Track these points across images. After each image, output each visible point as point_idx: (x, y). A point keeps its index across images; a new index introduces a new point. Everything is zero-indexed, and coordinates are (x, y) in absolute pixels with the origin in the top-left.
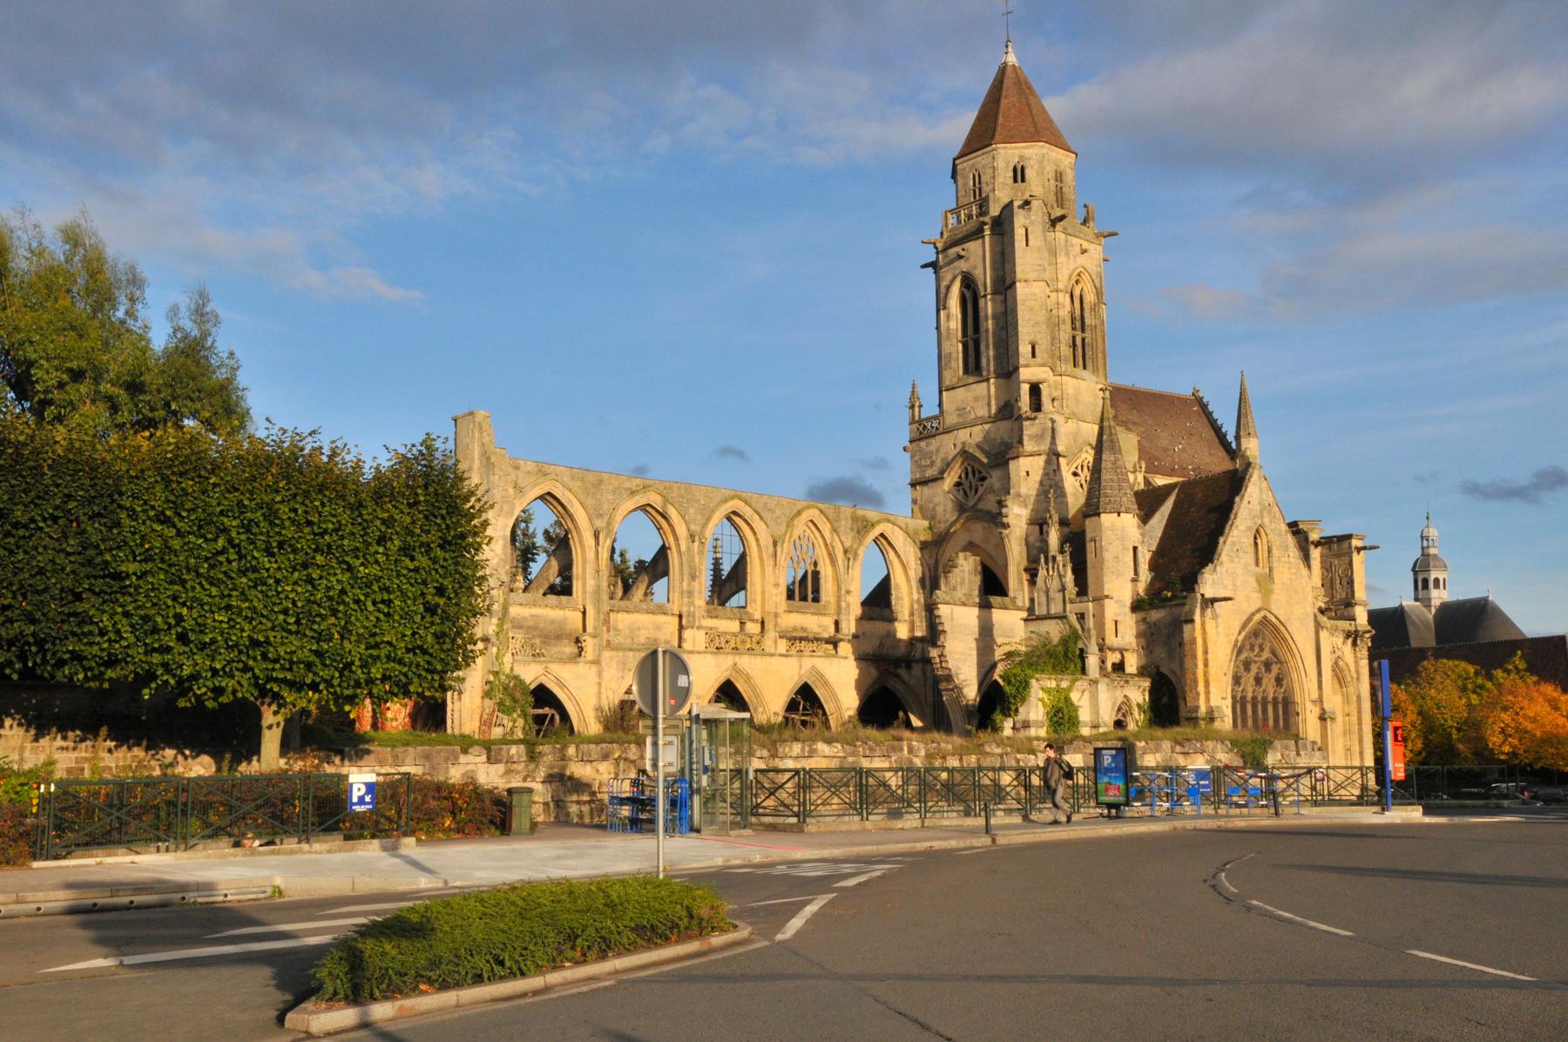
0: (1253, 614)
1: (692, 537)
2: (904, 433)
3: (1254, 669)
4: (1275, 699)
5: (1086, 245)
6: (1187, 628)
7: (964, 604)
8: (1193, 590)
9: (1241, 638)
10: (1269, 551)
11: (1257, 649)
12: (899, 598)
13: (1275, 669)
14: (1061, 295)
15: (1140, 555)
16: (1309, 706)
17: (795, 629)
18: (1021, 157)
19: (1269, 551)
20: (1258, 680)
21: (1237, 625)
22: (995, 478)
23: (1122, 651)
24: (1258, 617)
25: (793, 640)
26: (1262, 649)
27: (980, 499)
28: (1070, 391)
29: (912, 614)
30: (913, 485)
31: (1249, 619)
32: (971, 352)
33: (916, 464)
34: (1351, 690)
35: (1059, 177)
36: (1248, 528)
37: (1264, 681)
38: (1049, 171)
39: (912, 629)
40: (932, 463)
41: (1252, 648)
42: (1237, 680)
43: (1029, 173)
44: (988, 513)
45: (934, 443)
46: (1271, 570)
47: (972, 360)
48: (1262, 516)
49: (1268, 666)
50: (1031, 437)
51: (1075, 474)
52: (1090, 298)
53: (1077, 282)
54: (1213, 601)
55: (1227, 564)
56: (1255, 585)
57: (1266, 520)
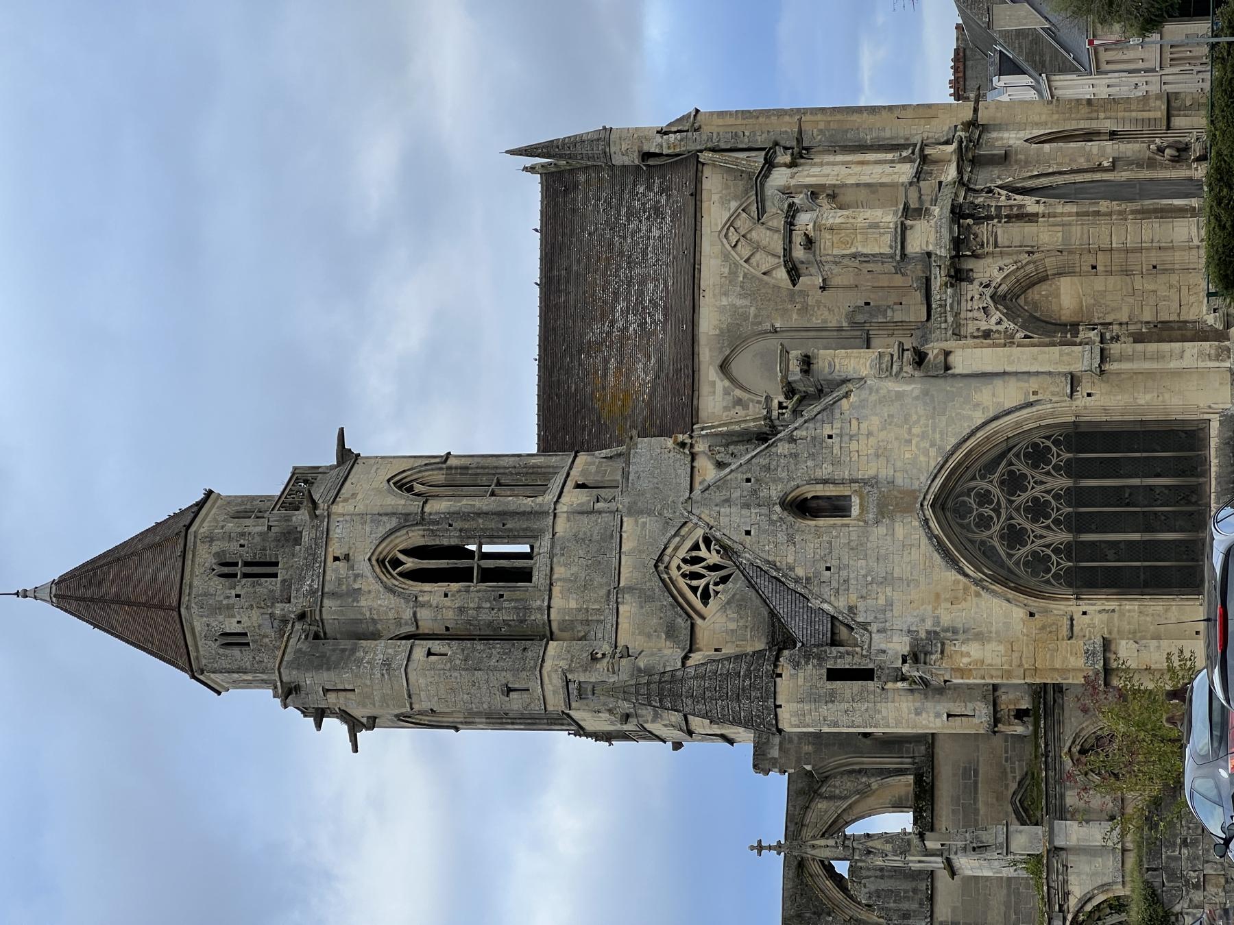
0: (931, 536)
3: (1021, 521)
4: (1070, 469)
5: (335, 549)
7: (931, 899)
9: (969, 570)
10: (825, 482)
11: (987, 511)
13: (1021, 467)
15: (840, 664)
16: (1081, 401)
19: (825, 482)
20: (1037, 510)
21: (952, 575)
24: (934, 524)
26: (984, 498)
28: (573, 604)
34: (1050, 263)
35: (227, 569)
36: (791, 540)
37: (1037, 491)
48: (768, 504)
49: (1014, 483)
52: (416, 538)
53: (396, 563)
55: (853, 599)
56: (882, 530)
57: (775, 492)
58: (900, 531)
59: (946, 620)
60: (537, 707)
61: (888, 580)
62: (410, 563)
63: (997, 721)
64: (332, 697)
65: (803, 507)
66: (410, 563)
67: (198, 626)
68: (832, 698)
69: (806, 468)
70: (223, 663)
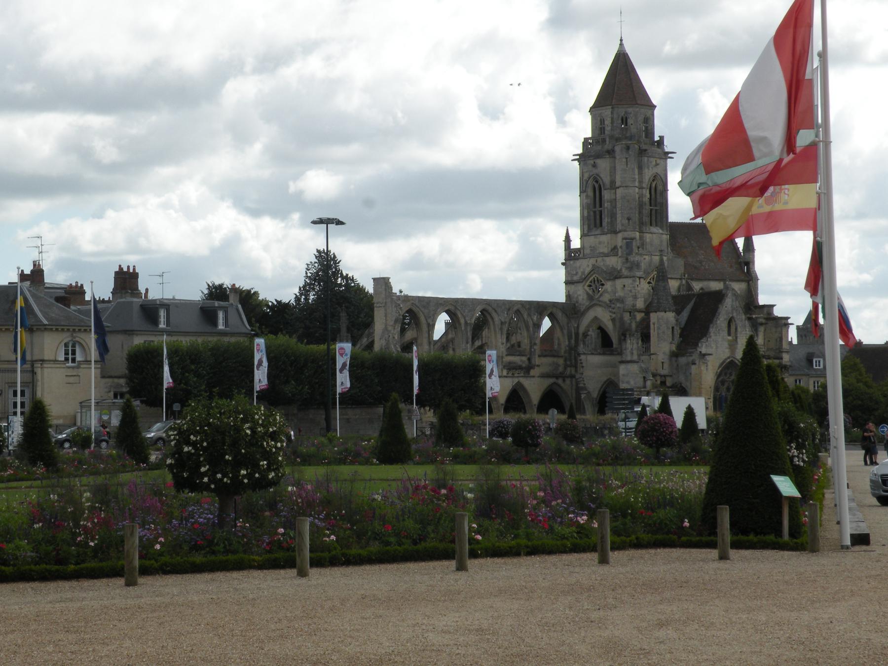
1: (466, 323)
2: (561, 255)
3: (726, 385)
5: (658, 161)
6: (693, 367)
7: (592, 354)
8: (696, 348)
10: (736, 329)
12: (559, 344)
14: (644, 191)
17: (510, 363)
18: (626, 112)
21: (718, 365)
22: (608, 286)
23: (665, 376)
25: (509, 369)
26: (731, 375)
27: (601, 295)
28: (648, 240)
29: (565, 352)
30: (567, 283)
31: (724, 362)
32: (598, 217)
33: (568, 273)
38: (641, 118)
39: (565, 360)
40: (577, 273)
41: (726, 374)
42: (717, 389)
43: (630, 121)
44: (605, 303)
45: (578, 263)
46: (736, 338)
47: (598, 221)
50: (627, 268)
51: (649, 283)
52: (660, 188)
54: (704, 355)
57: (735, 315)
58: (727, 350)
59: (709, 364)
60: (619, 227)
61: (717, 347)
62: (654, 185)
63: (661, 376)
64: (624, 160)
65: (730, 321)
66: (654, 185)
67: (630, 110)
68: (668, 328)
69: (740, 324)
70: (615, 116)
